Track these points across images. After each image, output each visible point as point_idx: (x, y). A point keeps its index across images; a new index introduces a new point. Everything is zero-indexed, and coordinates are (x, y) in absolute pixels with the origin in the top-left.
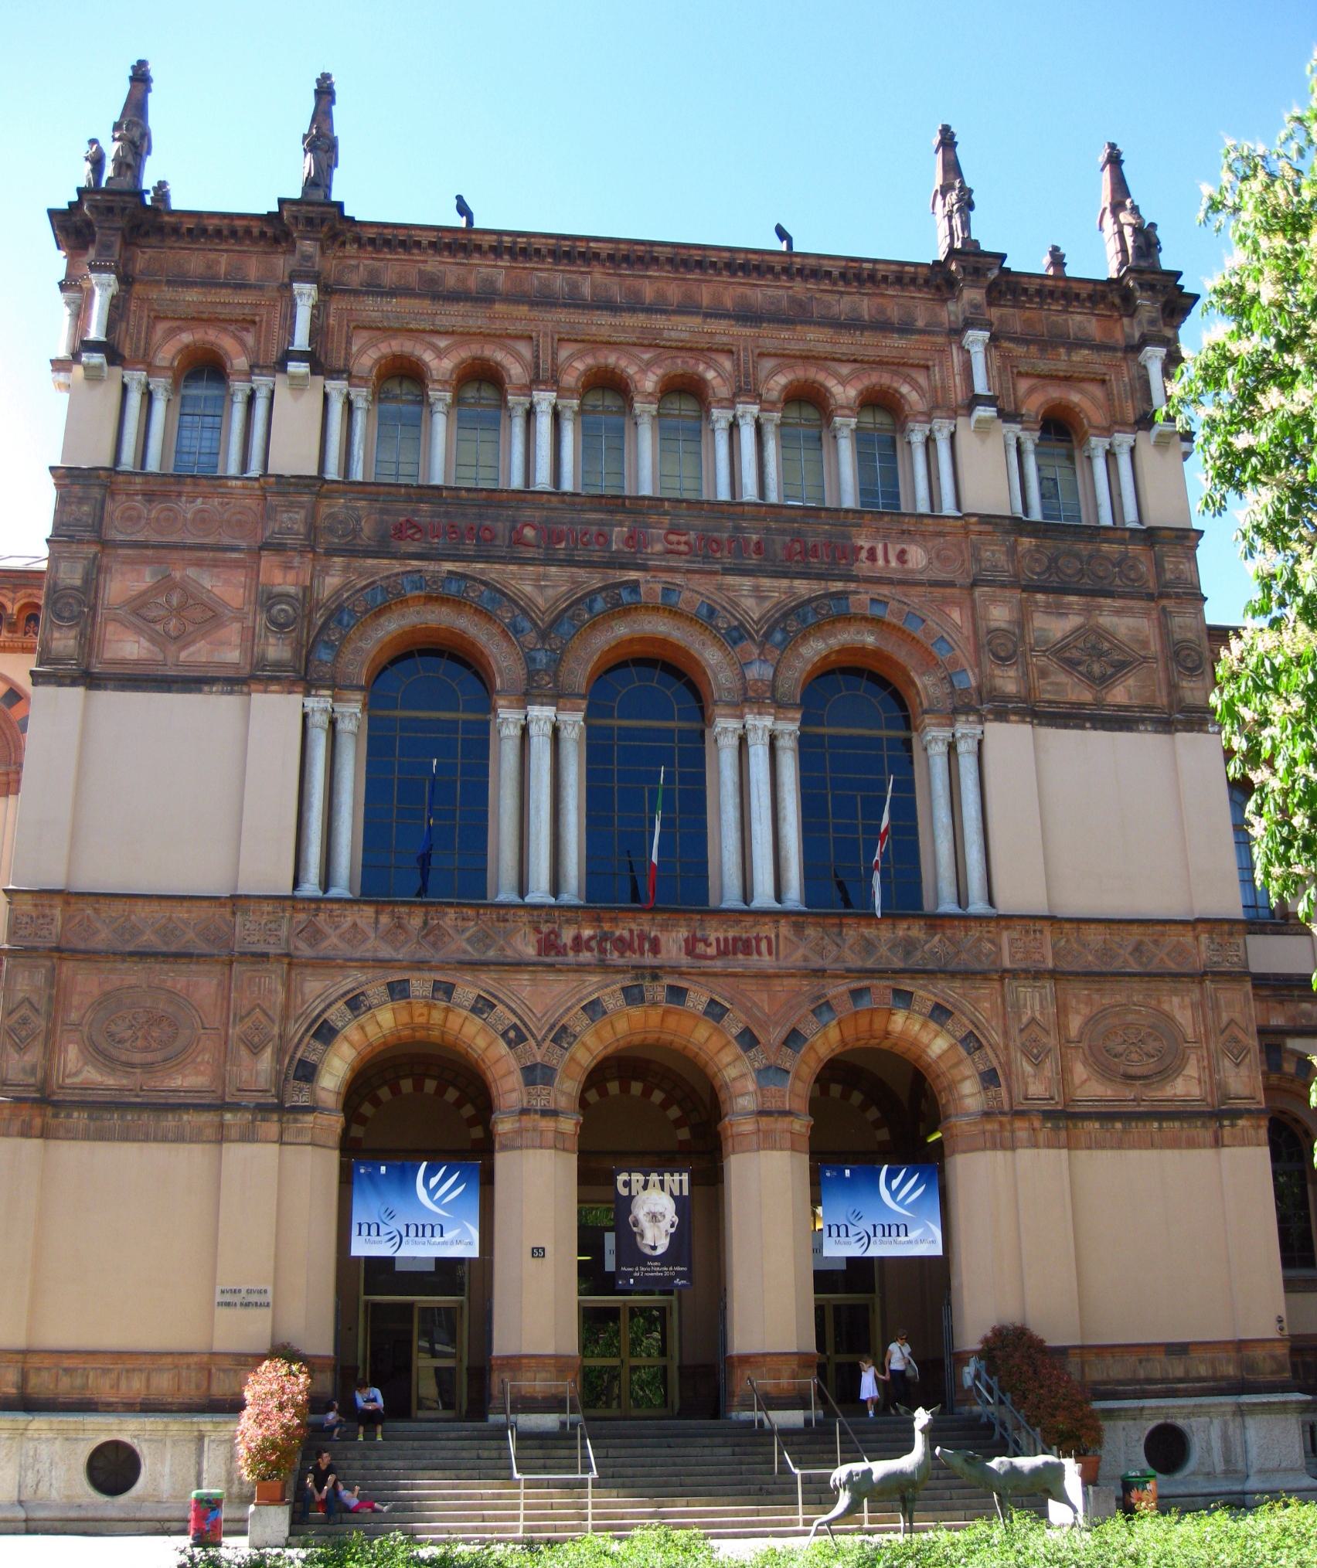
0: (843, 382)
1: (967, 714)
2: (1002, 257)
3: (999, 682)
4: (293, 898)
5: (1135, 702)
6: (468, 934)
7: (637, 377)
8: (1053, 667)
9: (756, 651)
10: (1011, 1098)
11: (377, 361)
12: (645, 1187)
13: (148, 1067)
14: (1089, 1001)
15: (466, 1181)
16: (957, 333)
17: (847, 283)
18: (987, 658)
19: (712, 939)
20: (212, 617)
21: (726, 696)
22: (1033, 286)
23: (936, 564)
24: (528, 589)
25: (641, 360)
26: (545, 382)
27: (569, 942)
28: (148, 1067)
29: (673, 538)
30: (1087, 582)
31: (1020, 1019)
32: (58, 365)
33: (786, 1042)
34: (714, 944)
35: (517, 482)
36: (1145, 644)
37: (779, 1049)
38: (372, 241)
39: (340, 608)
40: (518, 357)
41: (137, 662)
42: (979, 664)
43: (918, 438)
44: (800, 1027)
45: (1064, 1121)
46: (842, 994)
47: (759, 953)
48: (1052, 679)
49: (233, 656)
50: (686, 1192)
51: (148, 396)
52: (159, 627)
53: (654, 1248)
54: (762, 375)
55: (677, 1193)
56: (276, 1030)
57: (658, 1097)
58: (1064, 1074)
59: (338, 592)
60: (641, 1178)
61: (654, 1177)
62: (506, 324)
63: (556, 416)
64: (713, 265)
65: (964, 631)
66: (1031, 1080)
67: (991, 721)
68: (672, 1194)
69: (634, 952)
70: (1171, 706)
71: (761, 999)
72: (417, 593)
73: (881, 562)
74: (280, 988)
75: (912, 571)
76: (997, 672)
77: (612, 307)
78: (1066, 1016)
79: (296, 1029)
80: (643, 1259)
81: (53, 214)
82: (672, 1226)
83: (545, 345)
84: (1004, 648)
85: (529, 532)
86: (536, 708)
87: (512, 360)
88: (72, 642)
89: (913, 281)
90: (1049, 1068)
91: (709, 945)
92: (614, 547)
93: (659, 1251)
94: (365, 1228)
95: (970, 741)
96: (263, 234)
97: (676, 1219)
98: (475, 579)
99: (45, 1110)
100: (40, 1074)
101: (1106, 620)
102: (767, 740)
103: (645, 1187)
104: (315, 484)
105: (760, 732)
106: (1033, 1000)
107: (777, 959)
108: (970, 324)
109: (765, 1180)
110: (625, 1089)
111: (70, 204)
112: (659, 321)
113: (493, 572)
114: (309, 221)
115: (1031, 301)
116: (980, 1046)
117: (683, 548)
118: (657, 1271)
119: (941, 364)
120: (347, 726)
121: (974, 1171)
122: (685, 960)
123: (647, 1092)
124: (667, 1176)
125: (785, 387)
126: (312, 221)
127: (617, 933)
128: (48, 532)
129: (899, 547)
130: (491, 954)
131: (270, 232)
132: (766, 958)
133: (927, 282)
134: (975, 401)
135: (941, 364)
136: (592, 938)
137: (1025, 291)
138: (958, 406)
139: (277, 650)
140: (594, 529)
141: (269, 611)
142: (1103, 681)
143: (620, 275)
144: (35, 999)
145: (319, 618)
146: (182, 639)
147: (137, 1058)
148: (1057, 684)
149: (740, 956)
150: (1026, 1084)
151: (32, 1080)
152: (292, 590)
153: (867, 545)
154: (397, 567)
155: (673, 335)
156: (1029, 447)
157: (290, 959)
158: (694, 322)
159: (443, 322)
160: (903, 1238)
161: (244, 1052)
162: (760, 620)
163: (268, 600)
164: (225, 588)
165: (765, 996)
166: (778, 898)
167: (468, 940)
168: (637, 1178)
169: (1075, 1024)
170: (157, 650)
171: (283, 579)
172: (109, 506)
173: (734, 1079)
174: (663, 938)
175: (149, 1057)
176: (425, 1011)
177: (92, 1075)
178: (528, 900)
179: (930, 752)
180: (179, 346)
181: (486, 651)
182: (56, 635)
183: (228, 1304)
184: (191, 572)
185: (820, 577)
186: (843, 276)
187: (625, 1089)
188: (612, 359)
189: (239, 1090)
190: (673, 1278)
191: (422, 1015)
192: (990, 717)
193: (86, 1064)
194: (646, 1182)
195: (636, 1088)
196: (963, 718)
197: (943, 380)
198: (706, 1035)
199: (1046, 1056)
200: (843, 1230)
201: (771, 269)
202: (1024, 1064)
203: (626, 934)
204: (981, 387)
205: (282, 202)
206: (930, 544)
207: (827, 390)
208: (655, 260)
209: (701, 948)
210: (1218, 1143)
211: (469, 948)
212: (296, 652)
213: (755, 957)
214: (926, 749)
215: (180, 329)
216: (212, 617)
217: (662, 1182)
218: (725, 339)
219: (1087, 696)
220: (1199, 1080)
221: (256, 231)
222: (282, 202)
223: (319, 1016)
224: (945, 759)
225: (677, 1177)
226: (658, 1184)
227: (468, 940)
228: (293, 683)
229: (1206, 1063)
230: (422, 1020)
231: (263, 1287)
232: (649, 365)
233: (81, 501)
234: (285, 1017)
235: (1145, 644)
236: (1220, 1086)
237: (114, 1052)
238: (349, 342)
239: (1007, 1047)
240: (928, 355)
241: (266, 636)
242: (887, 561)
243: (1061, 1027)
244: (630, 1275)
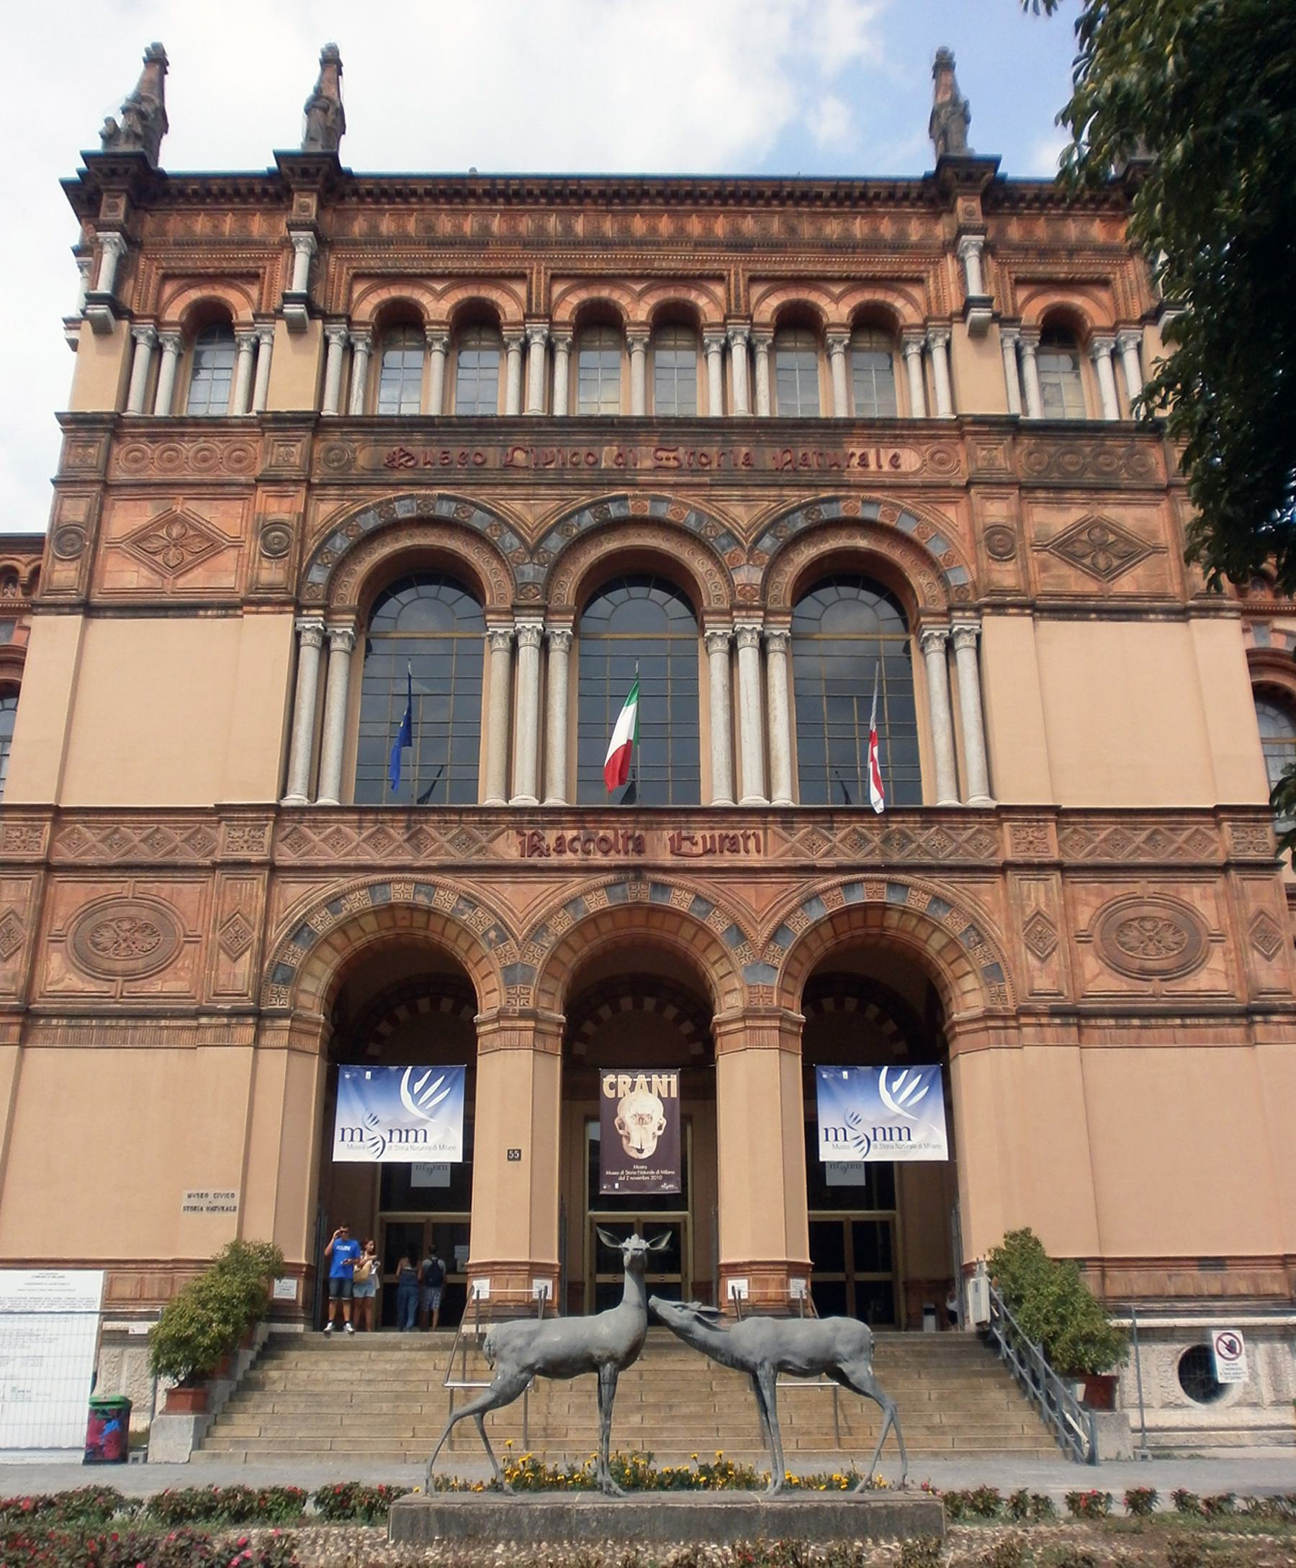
0: (837, 300)
1: (963, 609)
2: (994, 162)
3: (996, 577)
4: (277, 809)
5: (1144, 591)
6: (449, 836)
7: (629, 308)
8: (1055, 561)
9: (745, 558)
10: (1014, 992)
11: (376, 307)
12: (632, 1089)
13: (130, 976)
14: (1100, 894)
15: (452, 1085)
16: (952, 247)
17: (840, 204)
18: (984, 553)
19: (698, 838)
20: (212, 546)
21: (715, 605)
22: (1030, 194)
23: (930, 465)
24: (517, 506)
25: (634, 291)
26: (537, 316)
27: (553, 845)
28: (130, 976)
29: (660, 454)
30: (1090, 478)
31: (1023, 912)
32: (71, 323)
33: (773, 937)
34: (700, 842)
35: (511, 410)
36: (1154, 534)
37: (766, 944)
38: (370, 193)
39: (333, 533)
40: (514, 295)
41: (137, 591)
42: (976, 560)
43: (913, 350)
44: (789, 923)
45: (1075, 1017)
47: (747, 851)
48: (1054, 572)
49: (229, 581)
50: (674, 1094)
51: (157, 350)
52: (159, 558)
53: (641, 1151)
54: (753, 300)
55: (665, 1095)
56: (255, 934)
57: (671, 1012)
58: (1073, 967)
59: (331, 520)
60: (628, 1079)
61: (641, 1079)
62: (501, 264)
63: (550, 350)
64: (703, 195)
65: (960, 529)
66: (1036, 974)
67: (988, 615)
68: (659, 1096)
69: (618, 852)
70: (1184, 592)
71: (748, 895)
72: (409, 515)
73: (873, 467)
74: (260, 893)
75: (906, 474)
76: (996, 566)
77: (606, 244)
78: (1074, 908)
79: (277, 935)
80: (629, 1162)
81: (66, 185)
82: (660, 1128)
83: (539, 281)
84: (1000, 543)
85: (520, 456)
86: (523, 619)
87: (507, 297)
88: (73, 574)
89: (906, 196)
90: (1056, 961)
91: (696, 844)
92: (603, 466)
93: (645, 1155)
94: (348, 1134)
95: (966, 637)
96: (265, 192)
97: (664, 1122)
98: (465, 501)
99: (27, 1019)
100: (21, 982)
101: (1112, 513)
102: (756, 642)
103: (632, 1089)
104: (314, 423)
105: (749, 637)
106: (1040, 894)
107: (766, 854)
108: (963, 230)
109: (754, 1077)
110: (638, 1004)
111: (80, 173)
112: (650, 253)
113: (483, 496)
114: (305, 173)
115: (1029, 207)
116: (982, 941)
117: (673, 463)
118: (642, 1174)
119: (936, 277)
120: (338, 644)
121: (976, 1067)
122: (668, 860)
123: (660, 1008)
124: (655, 1078)
125: (778, 308)
126: (313, 176)
127: (601, 833)
128: (54, 472)
129: (891, 452)
130: (476, 859)
131: (271, 188)
132: (754, 855)
133: (920, 197)
134: (969, 303)
135: (936, 277)
136: (574, 839)
137: (1022, 198)
138: (952, 315)
139: (272, 573)
140: (584, 450)
141: (264, 537)
142: (1111, 573)
143: (611, 212)
144: (19, 910)
145: (312, 544)
146: (180, 569)
147: (119, 966)
148: (1059, 577)
149: (726, 853)
150: (1032, 978)
151: (13, 989)
152: (286, 517)
153: (858, 452)
154: (391, 494)
155: (664, 265)
156: (1029, 350)
157: (274, 869)
158: (684, 252)
159: (439, 266)
160: (905, 1142)
161: (223, 956)
162: (749, 529)
163: (266, 529)
164: (223, 517)
165: (753, 892)
166: (769, 796)
167: (450, 841)
168: (624, 1079)
169: (1084, 917)
170: (156, 577)
171: (281, 509)
172: (115, 450)
173: (722, 977)
174: (648, 836)
175: (131, 965)
176: (407, 914)
177: (75, 982)
178: (512, 803)
179: (927, 651)
180: (188, 301)
181: (478, 569)
182: (58, 567)
183: (195, 1208)
184: (192, 505)
185: (809, 486)
186: (834, 196)
187: (638, 1004)
188: (605, 293)
189: (215, 995)
190: (659, 1183)
191: (404, 918)
192: (988, 610)
193: (68, 971)
194: (634, 1084)
195: (650, 1003)
196: (959, 614)
197: (937, 290)
198: (692, 932)
199: (1054, 949)
200: (841, 1133)
201: (761, 195)
202: (1030, 957)
203: (610, 834)
204: (975, 290)
205: (279, 156)
207: (820, 308)
208: (645, 194)
210: (1250, 1041)
211: (451, 849)
212: (289, 575)
213: (742, 853)
214: (922, 650)
215: (190, 287)
216: (212, 546)
217: (649, 1084)
218: (716, 266)
219: (1091, 586)
220: (1226, 974)
221: (258, 189)
222: (279, 156)
223: (300, 920)
224: (943, 656)
225: (665, 1079)
226: (645, 1086)
227: (450, 841)
228: (284, 603)
229: (1233, 956)
230: (406, 923)
231: (231, 1192)
232: (642, 294)
233: (88, 444)
234: (266, 922)
235: (1154, 534)
236: (1247, 979)
237: (98, 961)
238: (350, 291)
239: (1010, 941)
240: (922, 268)
241: (260, 561)
242: (880, 467)
243: (1068, 919)
244: (613, 1180)
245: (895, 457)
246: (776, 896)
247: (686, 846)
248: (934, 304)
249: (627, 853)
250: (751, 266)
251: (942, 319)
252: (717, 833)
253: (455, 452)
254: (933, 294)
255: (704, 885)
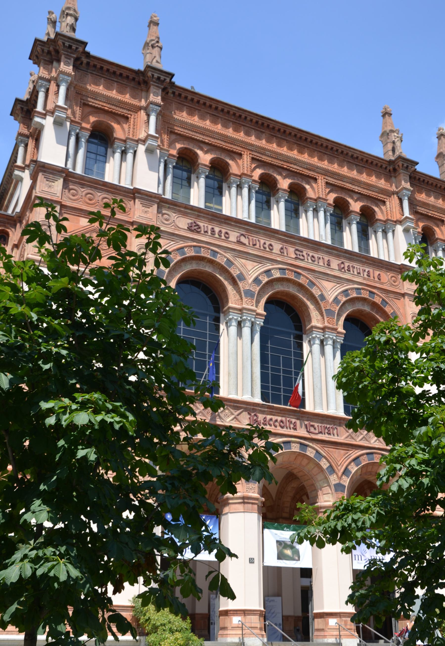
27: (262, 421)
29: (297, 252)
34: (317, 428)
46: (362, 455)
47: (334, 435)
122: (307, 435)
153: (367, 270)
206: (388, 274)
209: (312, 429)
245: (379, 275)
246: (344, 455)
247: (312, 429)
248: (389, 214)
249: (290, 429)
250: (326, 177)
251: (393, 221)
252: (323, 425)
253: (217, 230)
254: (389, 209)
255: (317, 447)
